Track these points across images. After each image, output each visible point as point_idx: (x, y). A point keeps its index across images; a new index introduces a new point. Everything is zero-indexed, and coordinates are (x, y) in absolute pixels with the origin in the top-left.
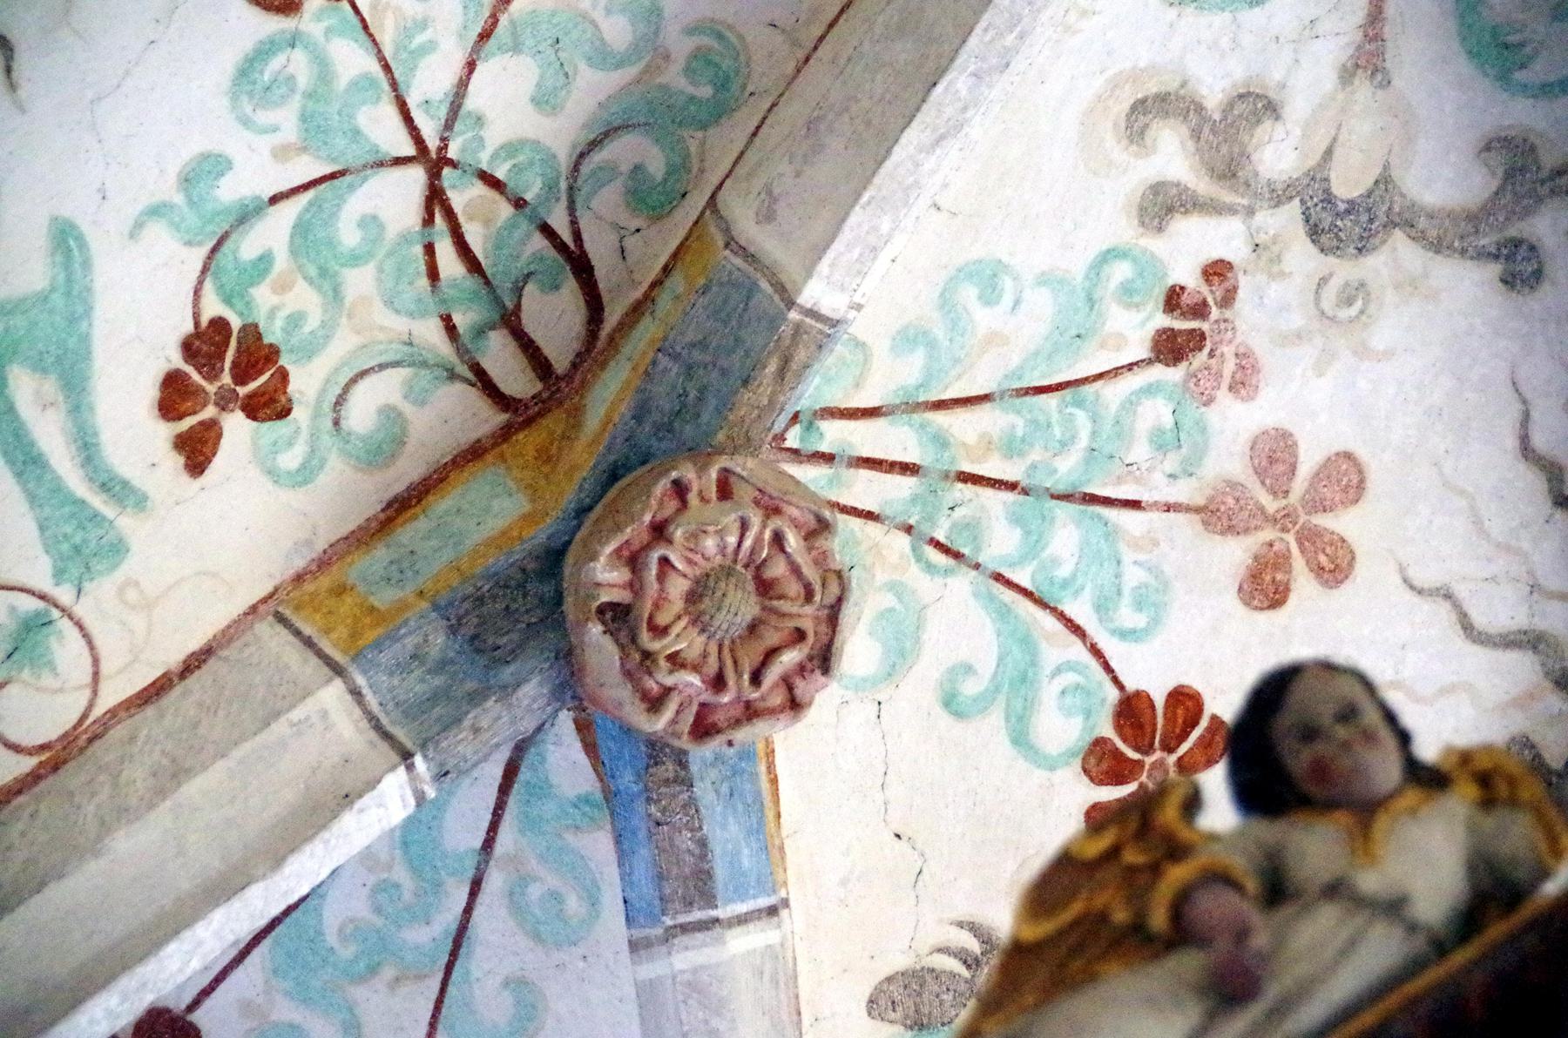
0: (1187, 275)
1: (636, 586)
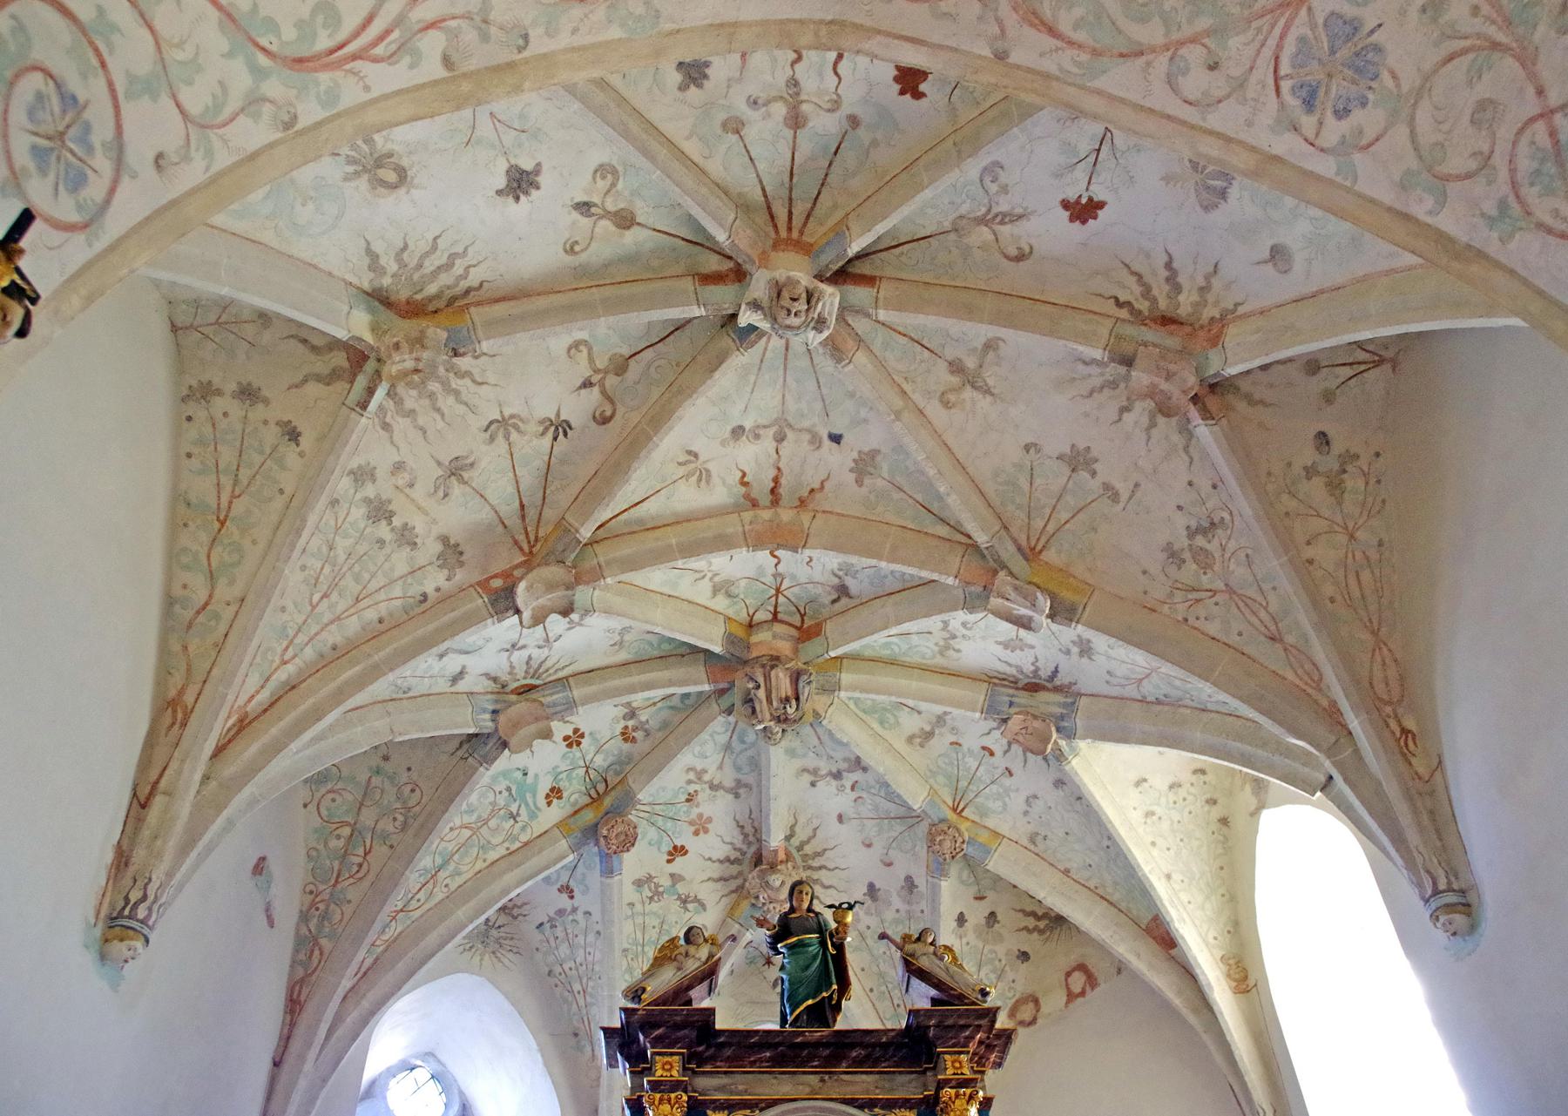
0: (692, 792)
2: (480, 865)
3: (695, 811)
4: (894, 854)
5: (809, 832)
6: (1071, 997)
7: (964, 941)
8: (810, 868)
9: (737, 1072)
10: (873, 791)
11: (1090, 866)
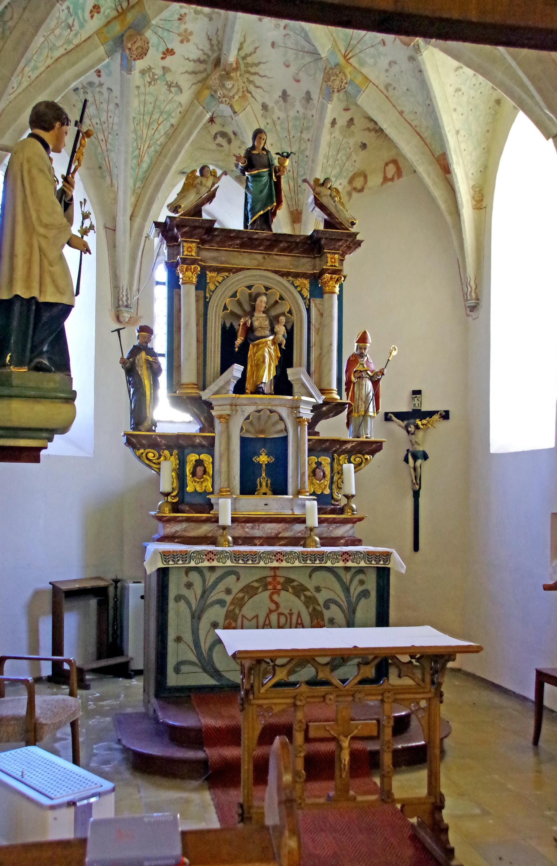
0: (183, 13)
1: (132, 47)
2: (49, 62)
3: (183, 27)
4: (302, 76)
5: (251, 49)
6: (386, 179)
7: (333, 136)
8: (248, 72)
9: (222, 250)
10: (297, 32)
11: (416, 113)
